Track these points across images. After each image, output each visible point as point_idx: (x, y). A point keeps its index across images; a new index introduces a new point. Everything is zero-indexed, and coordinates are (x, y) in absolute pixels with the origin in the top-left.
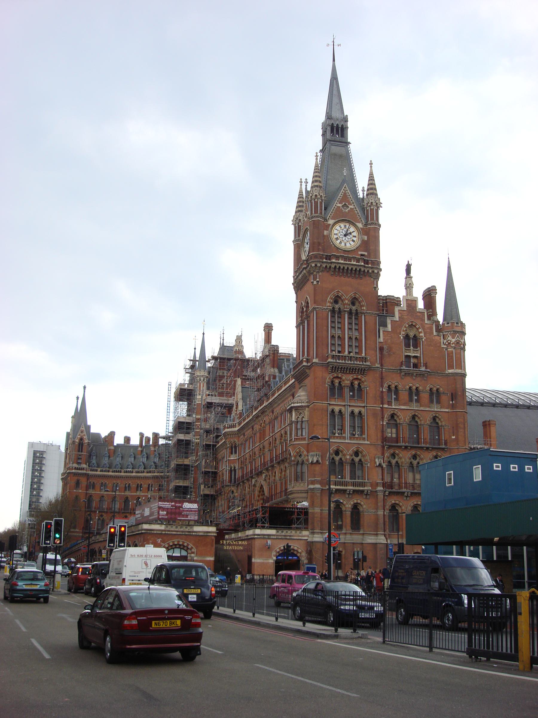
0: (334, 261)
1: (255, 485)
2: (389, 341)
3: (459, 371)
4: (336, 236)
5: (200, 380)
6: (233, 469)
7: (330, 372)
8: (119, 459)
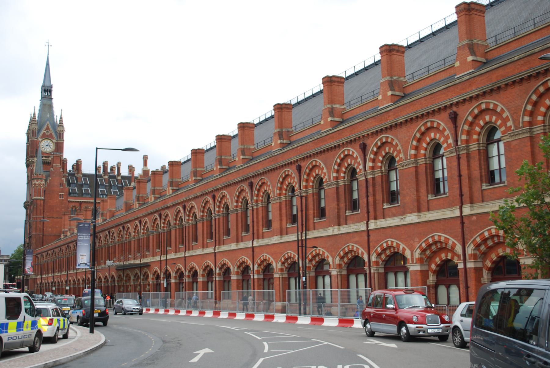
4: (42, 146)
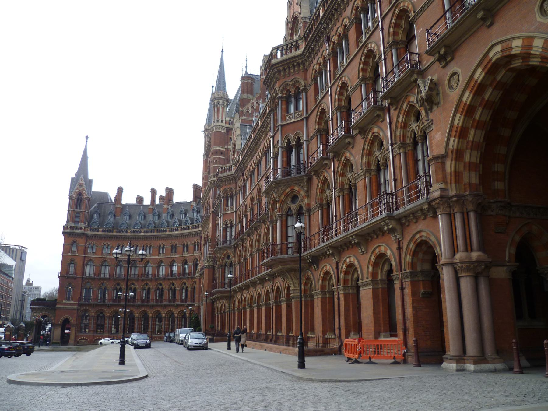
5: (219, 104)
6: (293, 143)
8: (126, 218)
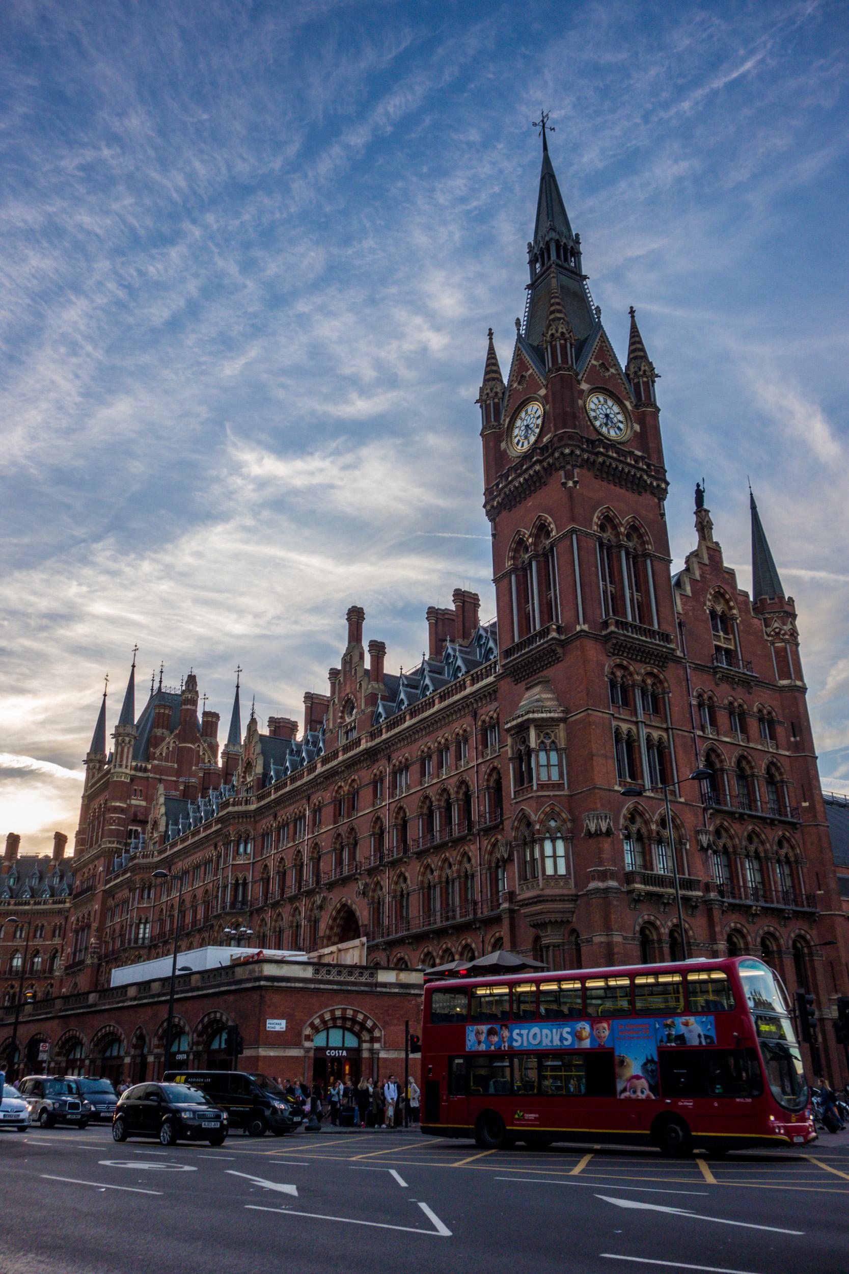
0: (602, 450)
1: (321, 908)
2: (691, 614)
3: (799, 683)
6: (240, 881)
7: (610, 652)
